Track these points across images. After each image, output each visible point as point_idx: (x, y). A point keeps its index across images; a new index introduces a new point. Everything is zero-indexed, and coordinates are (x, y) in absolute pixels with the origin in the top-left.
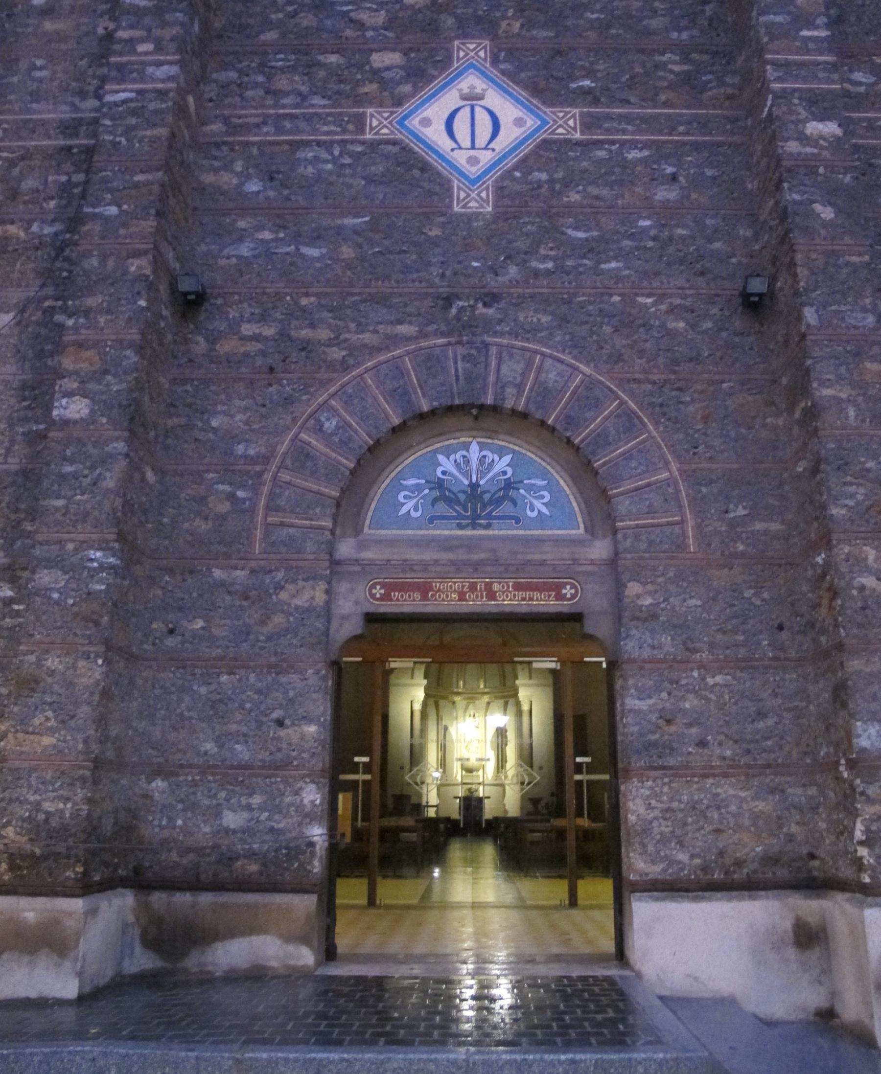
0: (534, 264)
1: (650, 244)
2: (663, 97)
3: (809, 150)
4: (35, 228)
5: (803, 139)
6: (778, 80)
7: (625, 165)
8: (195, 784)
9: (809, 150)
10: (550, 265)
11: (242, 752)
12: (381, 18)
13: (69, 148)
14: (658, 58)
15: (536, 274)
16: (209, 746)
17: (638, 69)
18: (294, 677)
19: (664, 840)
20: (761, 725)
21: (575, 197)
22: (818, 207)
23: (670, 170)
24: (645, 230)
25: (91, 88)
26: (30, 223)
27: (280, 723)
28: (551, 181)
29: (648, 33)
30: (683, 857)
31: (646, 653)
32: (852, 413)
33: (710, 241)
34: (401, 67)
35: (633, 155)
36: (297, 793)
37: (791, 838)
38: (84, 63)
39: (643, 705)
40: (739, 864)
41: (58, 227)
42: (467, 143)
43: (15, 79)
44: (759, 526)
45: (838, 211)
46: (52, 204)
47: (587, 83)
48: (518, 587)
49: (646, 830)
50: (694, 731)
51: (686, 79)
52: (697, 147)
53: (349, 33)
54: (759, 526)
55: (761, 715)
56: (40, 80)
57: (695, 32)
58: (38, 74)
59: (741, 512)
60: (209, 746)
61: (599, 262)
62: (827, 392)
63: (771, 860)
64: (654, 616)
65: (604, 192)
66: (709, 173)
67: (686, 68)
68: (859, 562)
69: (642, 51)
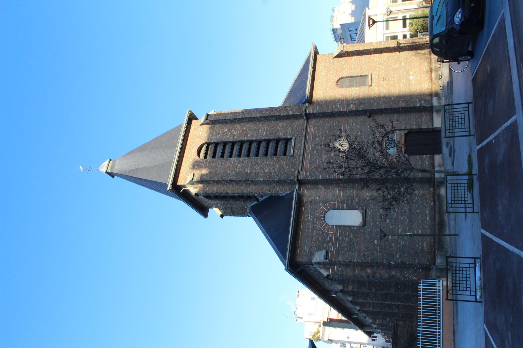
0: (363, 138)
1: (361, 126)
2: (341, 125)
3: (354, 107)
4: (354, 193)
5: (353, 108)
6: (345, 110)
7: (350, 129)
8: (424, 167)
9: (354, 107)
10: (364, 136)
11: (420, 163)
12: (326, 156)
13: (343, 190)
14: (335, 125)
15: (365, 137)
16: (419, 166)
17: (336, 127)
18: (412, 159)
19: (428, 125)
20: (417, 117)
21: (355, 134)
22: (362, 107)
23: (351, 124)
24: (359, 127)
25: (333, 189)
26: (353, 193)
27: (417, 160)
28: (352, 136)
29: (331, 126)
30: (430, 123)
31: (409, 127)
32: (386, 105)
33: (361, 120)
34: (334, 153)
35: (349, 128)
36: (424, 157)
37: (428, 114)
38: (329, 191)
39: (415, 127)
40: (430, 119)
41: (355, 190)
42: (346, 145)
43: (331, 199)
44: (396, 116)
45: (362, 105)
46: (351, 191)
47: (338, 133)
48: (402, 139)
49: (427, 127)
50: (417, 123)
51: (338, 122)
52: (348, 121)
53: (328, 159)
54: (396, 116)
55: (416, 117)
56: (331, 196)
57: (331, 121)
58: (330, 196)
59: (394, 118)
60: (419, 166)
61: (363, 131)
62: (383, 107)
63: (430, 116)
64: (405, 126)
65: (354, 131)
66: (352, 120)
67: (336, 122)
68: (401, 105)
69: (333, 127)
